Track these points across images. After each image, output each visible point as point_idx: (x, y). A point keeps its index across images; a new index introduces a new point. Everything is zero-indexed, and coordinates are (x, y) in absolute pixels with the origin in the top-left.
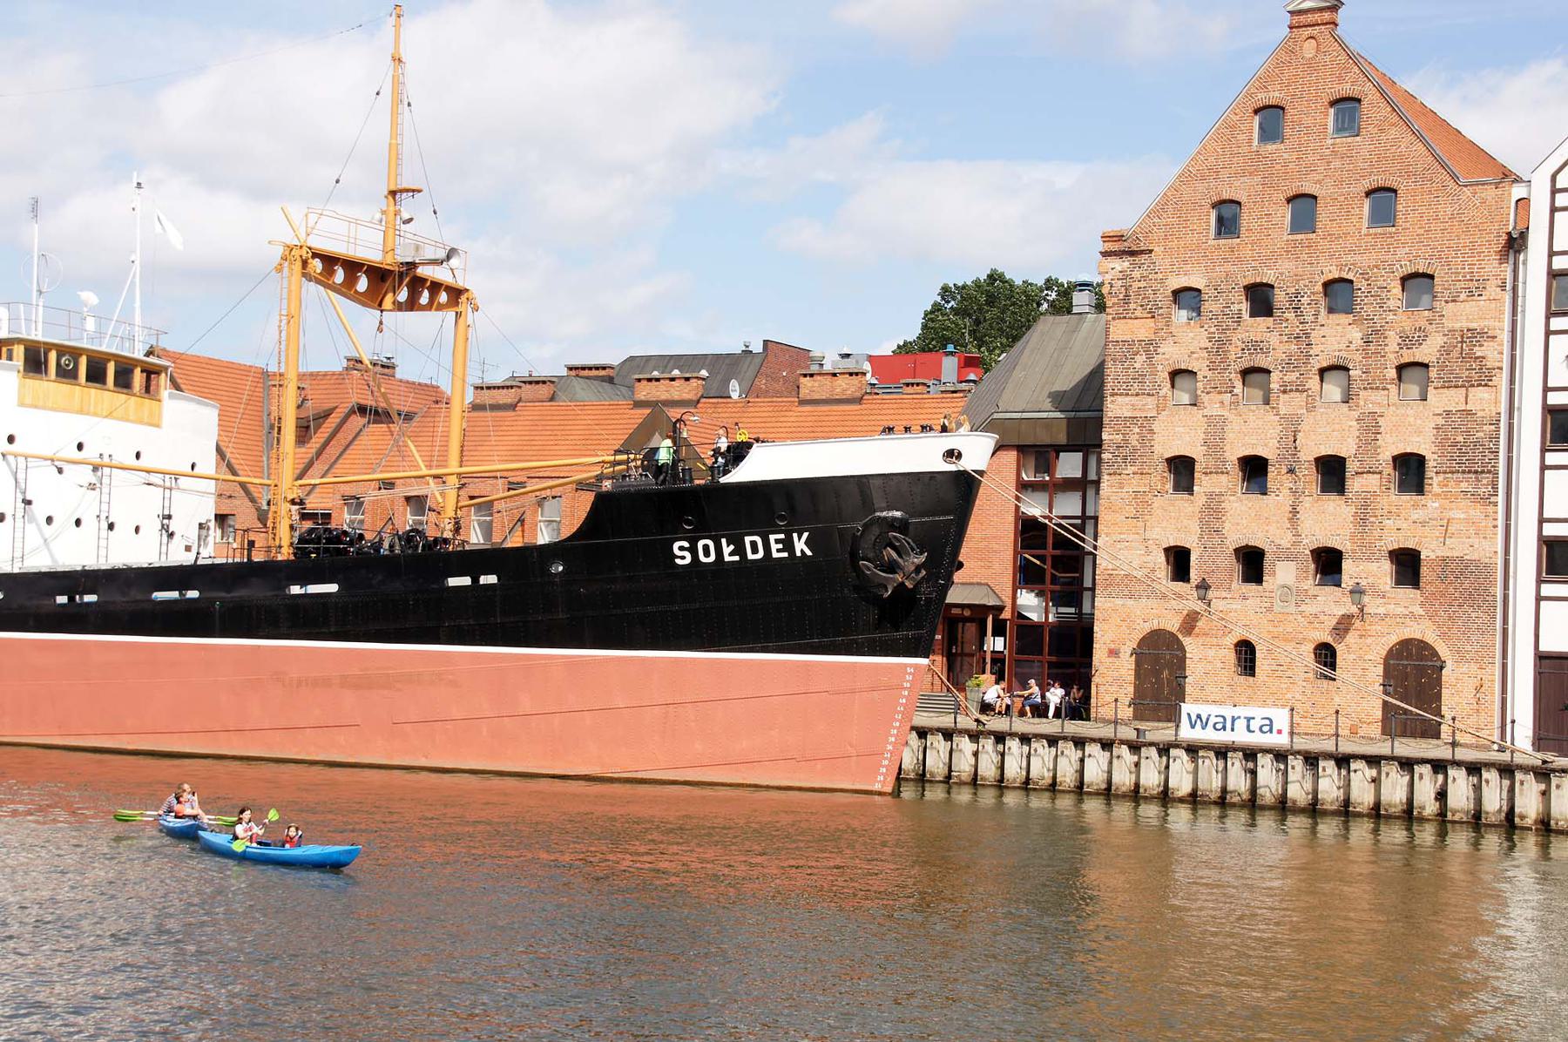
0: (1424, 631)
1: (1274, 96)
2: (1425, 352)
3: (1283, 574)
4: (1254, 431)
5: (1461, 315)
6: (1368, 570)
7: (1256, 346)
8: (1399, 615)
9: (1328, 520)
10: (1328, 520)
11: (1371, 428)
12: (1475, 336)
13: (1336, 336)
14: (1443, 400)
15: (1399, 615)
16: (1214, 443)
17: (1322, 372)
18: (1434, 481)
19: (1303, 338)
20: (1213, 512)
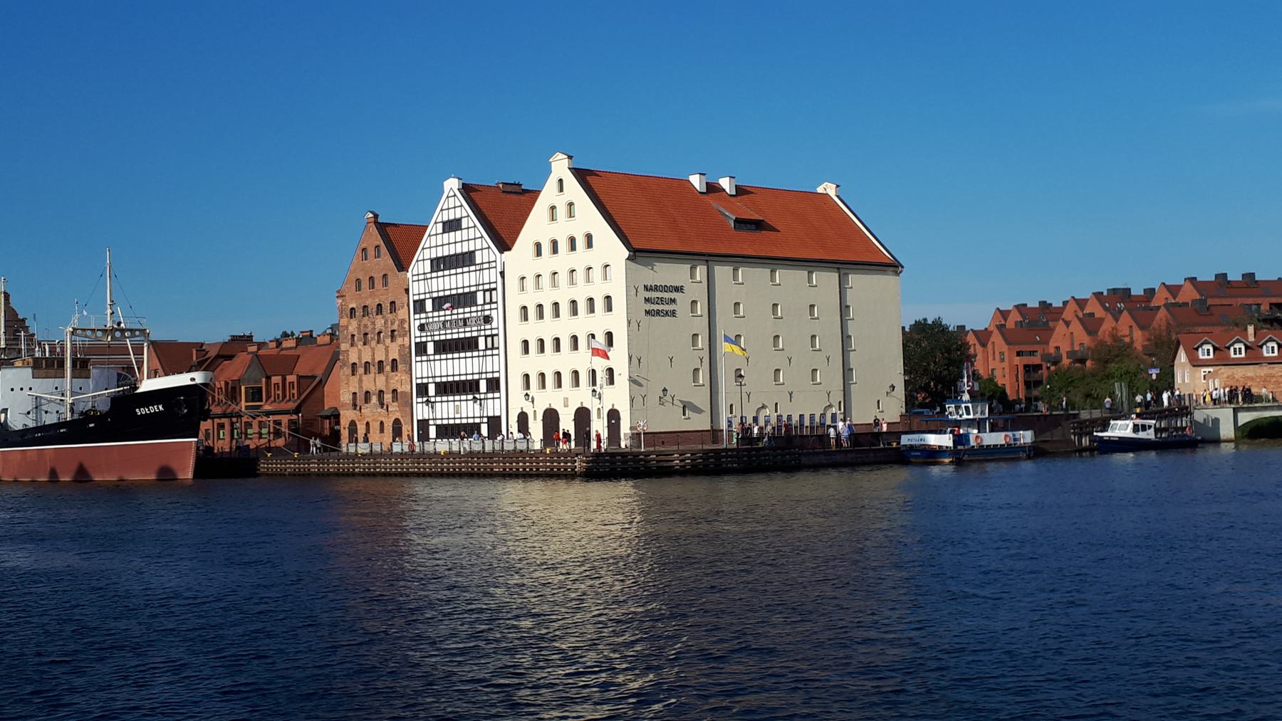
0: (398, 415)
1: (364, 246)
2: (395, 327)
3: (374, 399)
4: (367, 357)
5: (402, 313)
6: (388, 397)
7: (366, 326)
8: (395, 411)
9: (381, 382)
10: (381, 382)
11: (387, 351)
12: (403, 321)
13: (380, 322)
14: (399, 341)
15: (395, 411)
16: (360, 358)
17: (379, 333)
18: (399, 366)
19: (373, 323)
20: (361, 381)
